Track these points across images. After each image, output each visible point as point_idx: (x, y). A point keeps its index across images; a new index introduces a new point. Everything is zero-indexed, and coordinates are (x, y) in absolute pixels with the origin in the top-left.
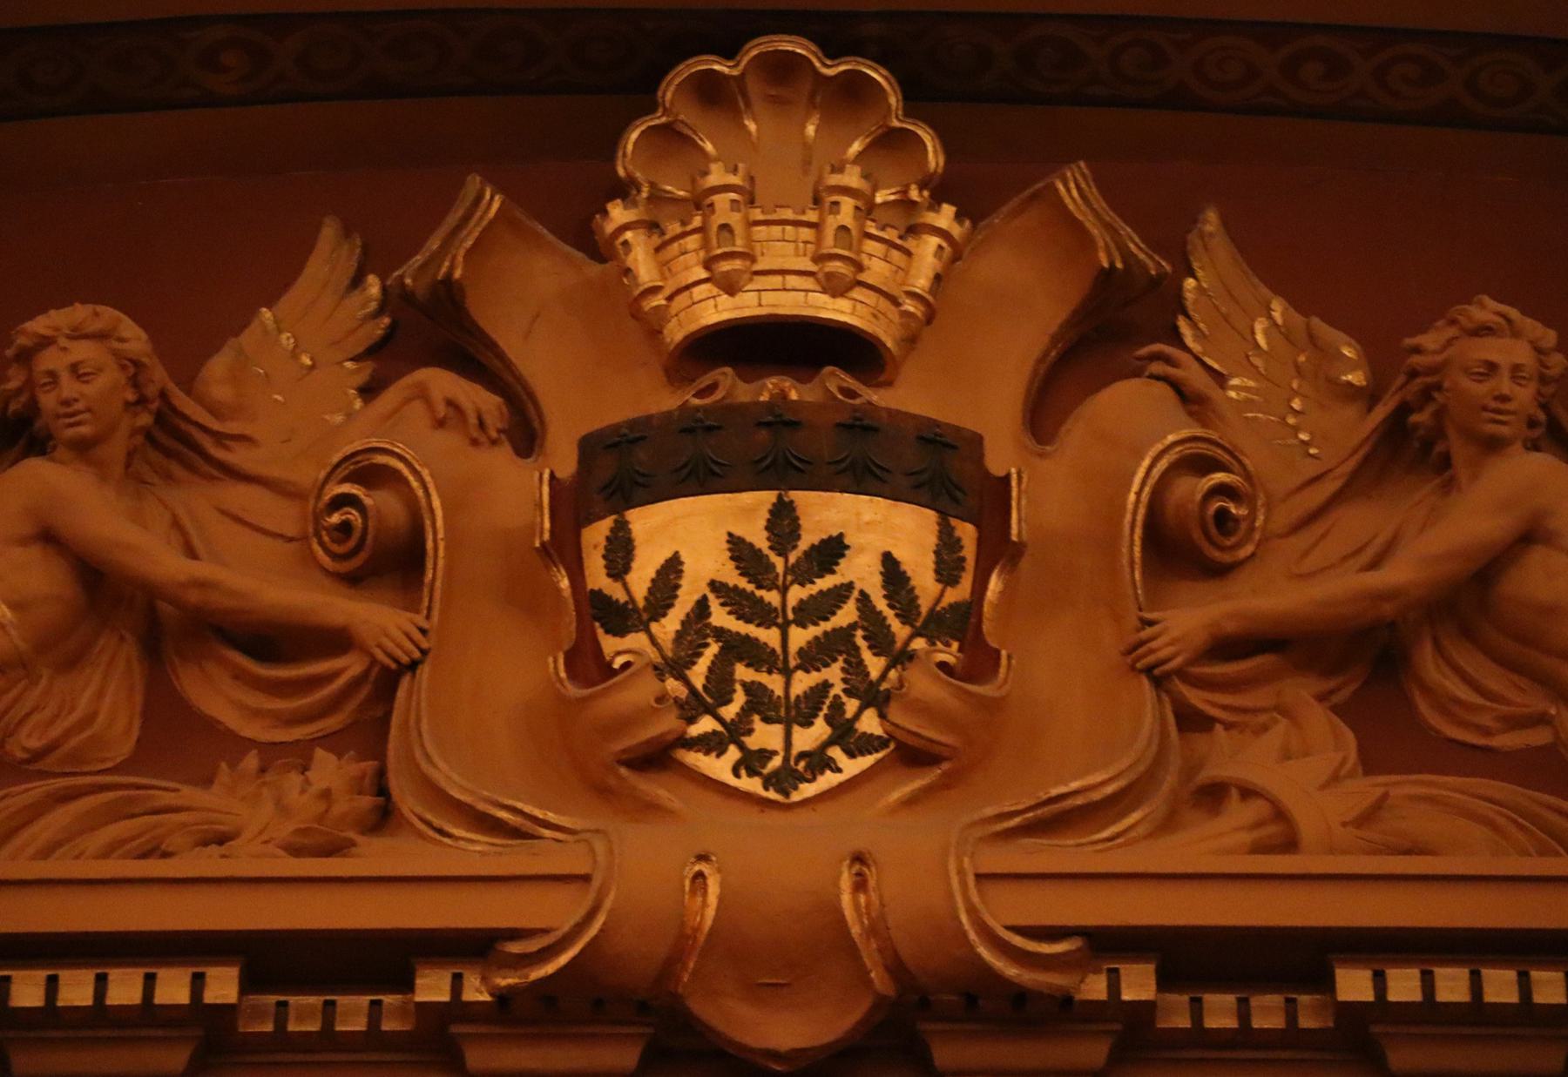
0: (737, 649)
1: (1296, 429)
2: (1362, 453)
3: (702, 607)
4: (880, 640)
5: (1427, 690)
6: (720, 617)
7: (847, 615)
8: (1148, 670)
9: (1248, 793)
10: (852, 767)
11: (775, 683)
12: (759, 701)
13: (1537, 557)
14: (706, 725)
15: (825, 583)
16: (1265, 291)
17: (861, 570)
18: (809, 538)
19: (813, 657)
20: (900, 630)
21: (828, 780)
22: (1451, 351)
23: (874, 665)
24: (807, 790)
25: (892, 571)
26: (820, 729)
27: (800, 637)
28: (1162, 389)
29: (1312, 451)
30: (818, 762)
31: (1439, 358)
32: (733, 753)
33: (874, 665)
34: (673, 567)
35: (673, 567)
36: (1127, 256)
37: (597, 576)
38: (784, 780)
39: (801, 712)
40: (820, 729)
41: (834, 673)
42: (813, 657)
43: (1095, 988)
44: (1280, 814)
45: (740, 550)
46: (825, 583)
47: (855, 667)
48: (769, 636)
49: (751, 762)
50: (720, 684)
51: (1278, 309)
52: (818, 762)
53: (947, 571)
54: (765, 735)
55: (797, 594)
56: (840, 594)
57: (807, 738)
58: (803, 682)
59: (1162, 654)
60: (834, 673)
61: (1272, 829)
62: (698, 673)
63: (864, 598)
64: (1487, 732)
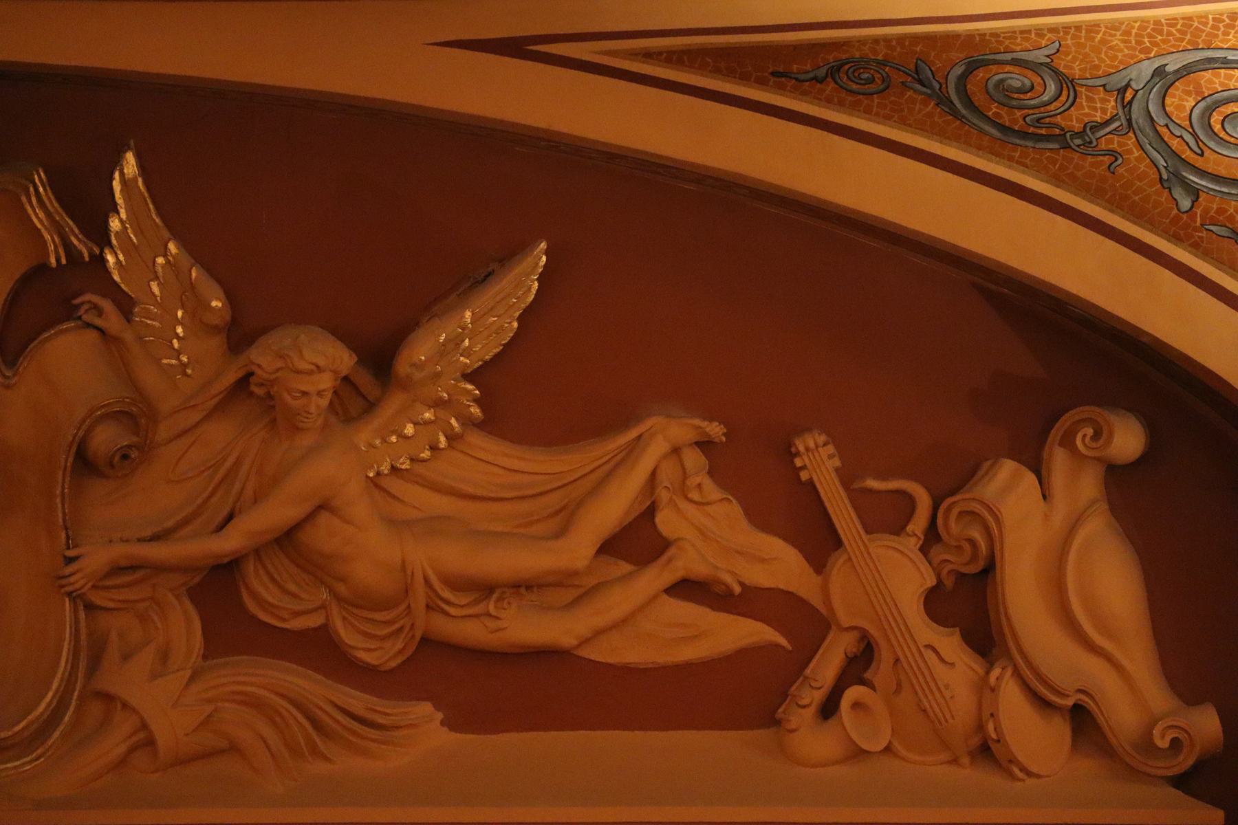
1: (179, 353)
2: (221, 396)
5: (247, 588)
8: (69, 594)
9: (125, 705)
13: (324, 518)
16: (167, 234)
22: (278, 374)
28: (92, 335)
29: (189, 371)
31: (273, 376)
36: (68, 247)
44: (144, 726)
51: (172, 247)
59: (77, 586)
61: (142, 735)
64: (284, 620)
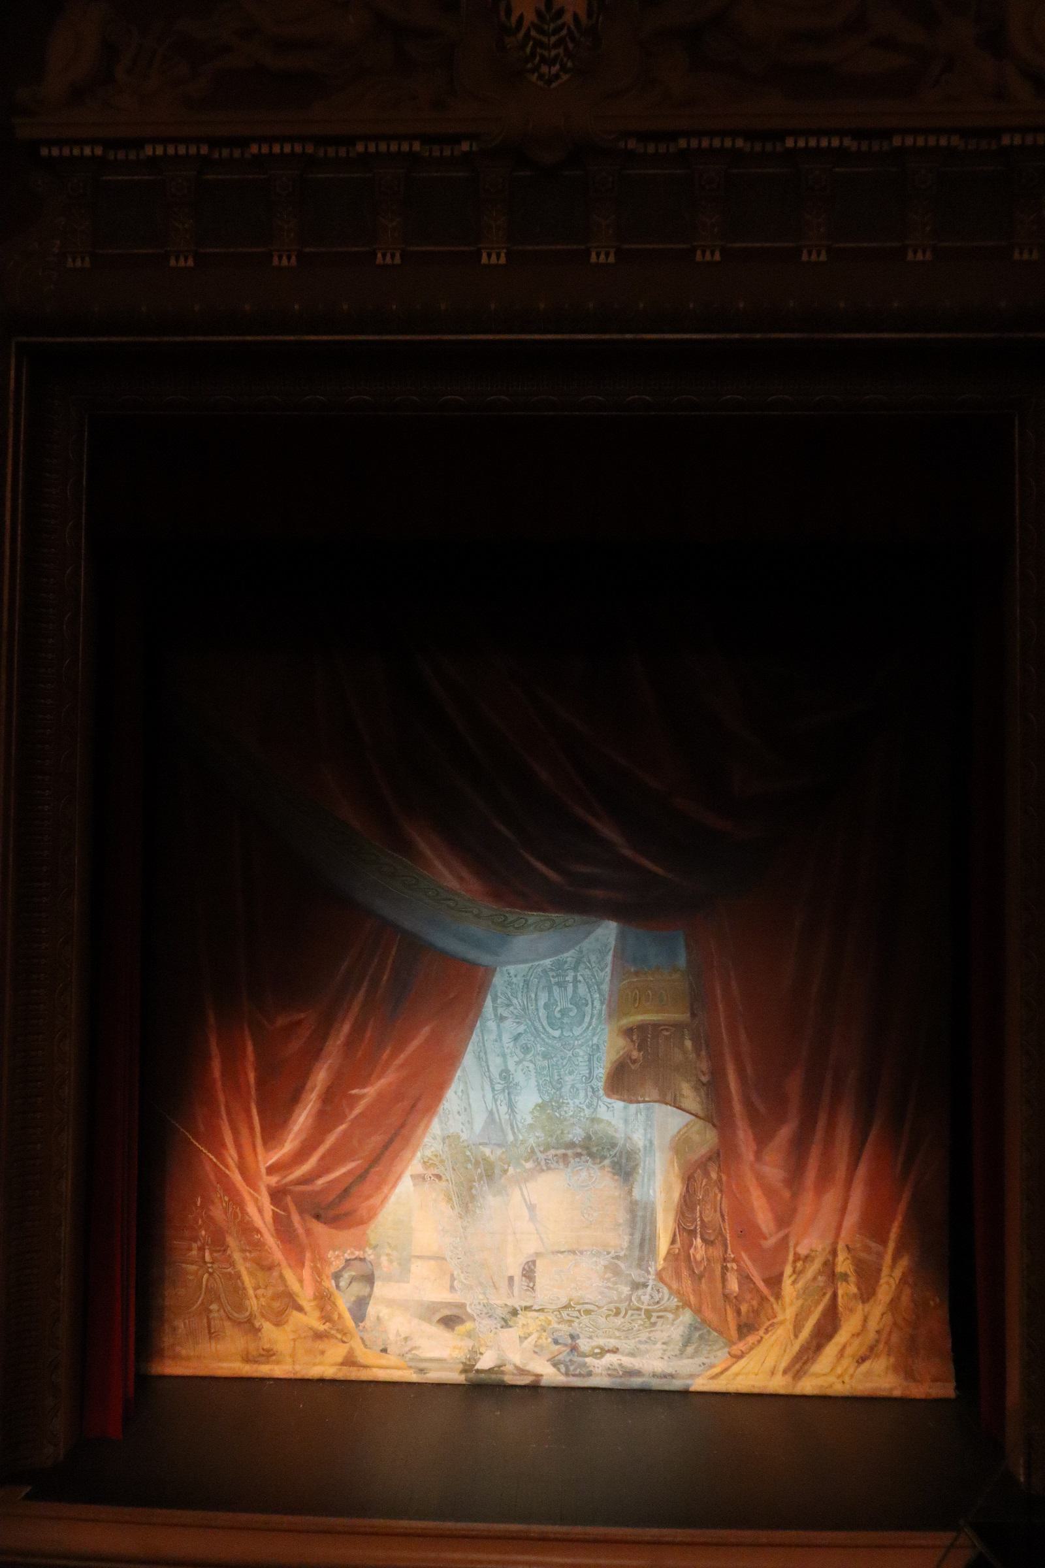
0: (539, 44)
3: (529, 29)
4: (573, 39)
6: (533, 33)
7: (564, 32)
10: (565, 77)
11: (546, 53)
12: (543, 60)
14: (529, 66)
15: (560, 22)
17: (568, 18)
18: (556, 7)
19: (556, 46)
20: (577, 35)
21: (560, 81)
23: (571, 46)
24: (554, 85)
25: (576, 17)
26: (557, 67)
27: (553, 39)
30: (557, 76)
32: (536, 75)
33: (571, 46)
34: (521, 17)
35: (521, 17)
37: (503, 18)
38: (549, 82)
39: (551, 62)
40: (557, 67)
41: (561, 50)
42: (556, 46)
43: (622, 145)
45: (539, 14)
46: (560, 22)
47: (566, 49)
48: (545, 39)
49: (541, 77)
50: (533, 54)
52: (557, 76)
53: (590, 16)
54: (544, 69)
55: (552, 26)
56: (564, 25)
57: (555, 69)
58: (553, 53)
60: (561, 50)
62: (528, 50)
63: (569, 28)
